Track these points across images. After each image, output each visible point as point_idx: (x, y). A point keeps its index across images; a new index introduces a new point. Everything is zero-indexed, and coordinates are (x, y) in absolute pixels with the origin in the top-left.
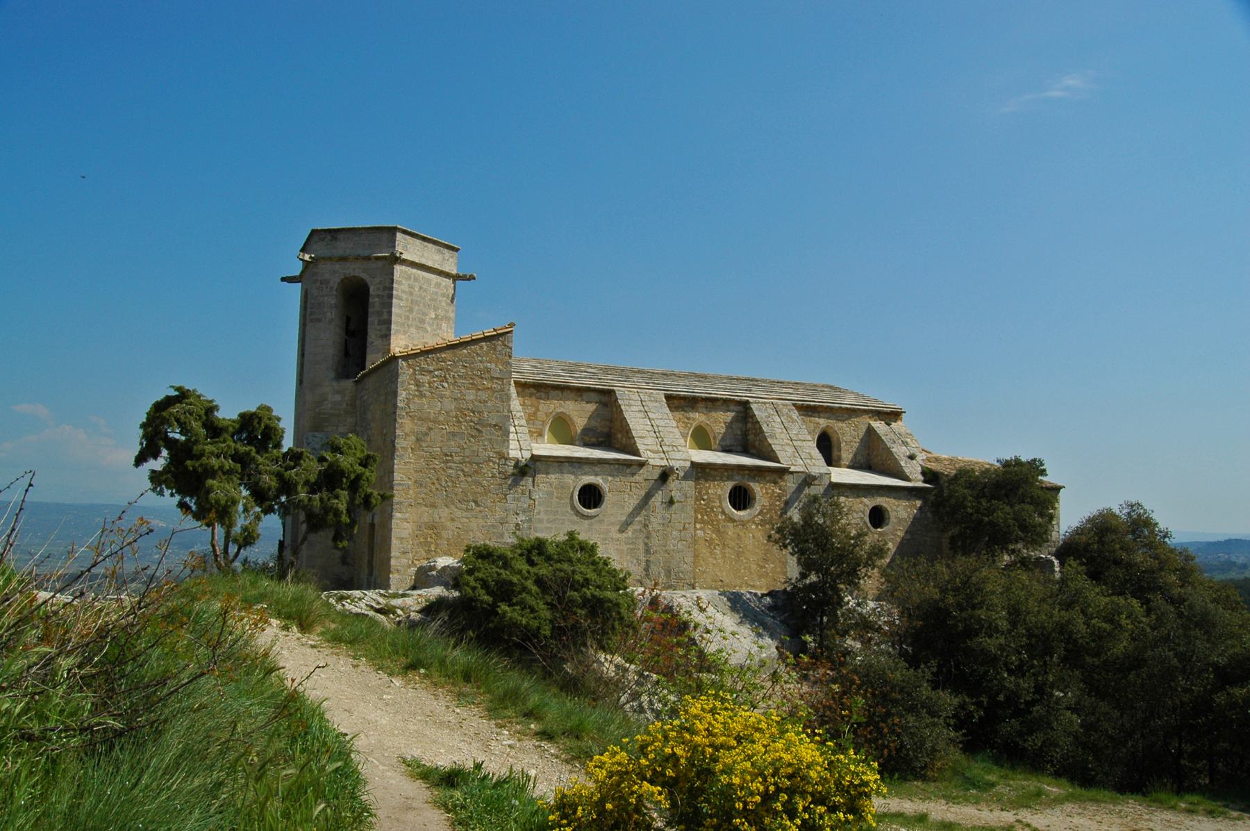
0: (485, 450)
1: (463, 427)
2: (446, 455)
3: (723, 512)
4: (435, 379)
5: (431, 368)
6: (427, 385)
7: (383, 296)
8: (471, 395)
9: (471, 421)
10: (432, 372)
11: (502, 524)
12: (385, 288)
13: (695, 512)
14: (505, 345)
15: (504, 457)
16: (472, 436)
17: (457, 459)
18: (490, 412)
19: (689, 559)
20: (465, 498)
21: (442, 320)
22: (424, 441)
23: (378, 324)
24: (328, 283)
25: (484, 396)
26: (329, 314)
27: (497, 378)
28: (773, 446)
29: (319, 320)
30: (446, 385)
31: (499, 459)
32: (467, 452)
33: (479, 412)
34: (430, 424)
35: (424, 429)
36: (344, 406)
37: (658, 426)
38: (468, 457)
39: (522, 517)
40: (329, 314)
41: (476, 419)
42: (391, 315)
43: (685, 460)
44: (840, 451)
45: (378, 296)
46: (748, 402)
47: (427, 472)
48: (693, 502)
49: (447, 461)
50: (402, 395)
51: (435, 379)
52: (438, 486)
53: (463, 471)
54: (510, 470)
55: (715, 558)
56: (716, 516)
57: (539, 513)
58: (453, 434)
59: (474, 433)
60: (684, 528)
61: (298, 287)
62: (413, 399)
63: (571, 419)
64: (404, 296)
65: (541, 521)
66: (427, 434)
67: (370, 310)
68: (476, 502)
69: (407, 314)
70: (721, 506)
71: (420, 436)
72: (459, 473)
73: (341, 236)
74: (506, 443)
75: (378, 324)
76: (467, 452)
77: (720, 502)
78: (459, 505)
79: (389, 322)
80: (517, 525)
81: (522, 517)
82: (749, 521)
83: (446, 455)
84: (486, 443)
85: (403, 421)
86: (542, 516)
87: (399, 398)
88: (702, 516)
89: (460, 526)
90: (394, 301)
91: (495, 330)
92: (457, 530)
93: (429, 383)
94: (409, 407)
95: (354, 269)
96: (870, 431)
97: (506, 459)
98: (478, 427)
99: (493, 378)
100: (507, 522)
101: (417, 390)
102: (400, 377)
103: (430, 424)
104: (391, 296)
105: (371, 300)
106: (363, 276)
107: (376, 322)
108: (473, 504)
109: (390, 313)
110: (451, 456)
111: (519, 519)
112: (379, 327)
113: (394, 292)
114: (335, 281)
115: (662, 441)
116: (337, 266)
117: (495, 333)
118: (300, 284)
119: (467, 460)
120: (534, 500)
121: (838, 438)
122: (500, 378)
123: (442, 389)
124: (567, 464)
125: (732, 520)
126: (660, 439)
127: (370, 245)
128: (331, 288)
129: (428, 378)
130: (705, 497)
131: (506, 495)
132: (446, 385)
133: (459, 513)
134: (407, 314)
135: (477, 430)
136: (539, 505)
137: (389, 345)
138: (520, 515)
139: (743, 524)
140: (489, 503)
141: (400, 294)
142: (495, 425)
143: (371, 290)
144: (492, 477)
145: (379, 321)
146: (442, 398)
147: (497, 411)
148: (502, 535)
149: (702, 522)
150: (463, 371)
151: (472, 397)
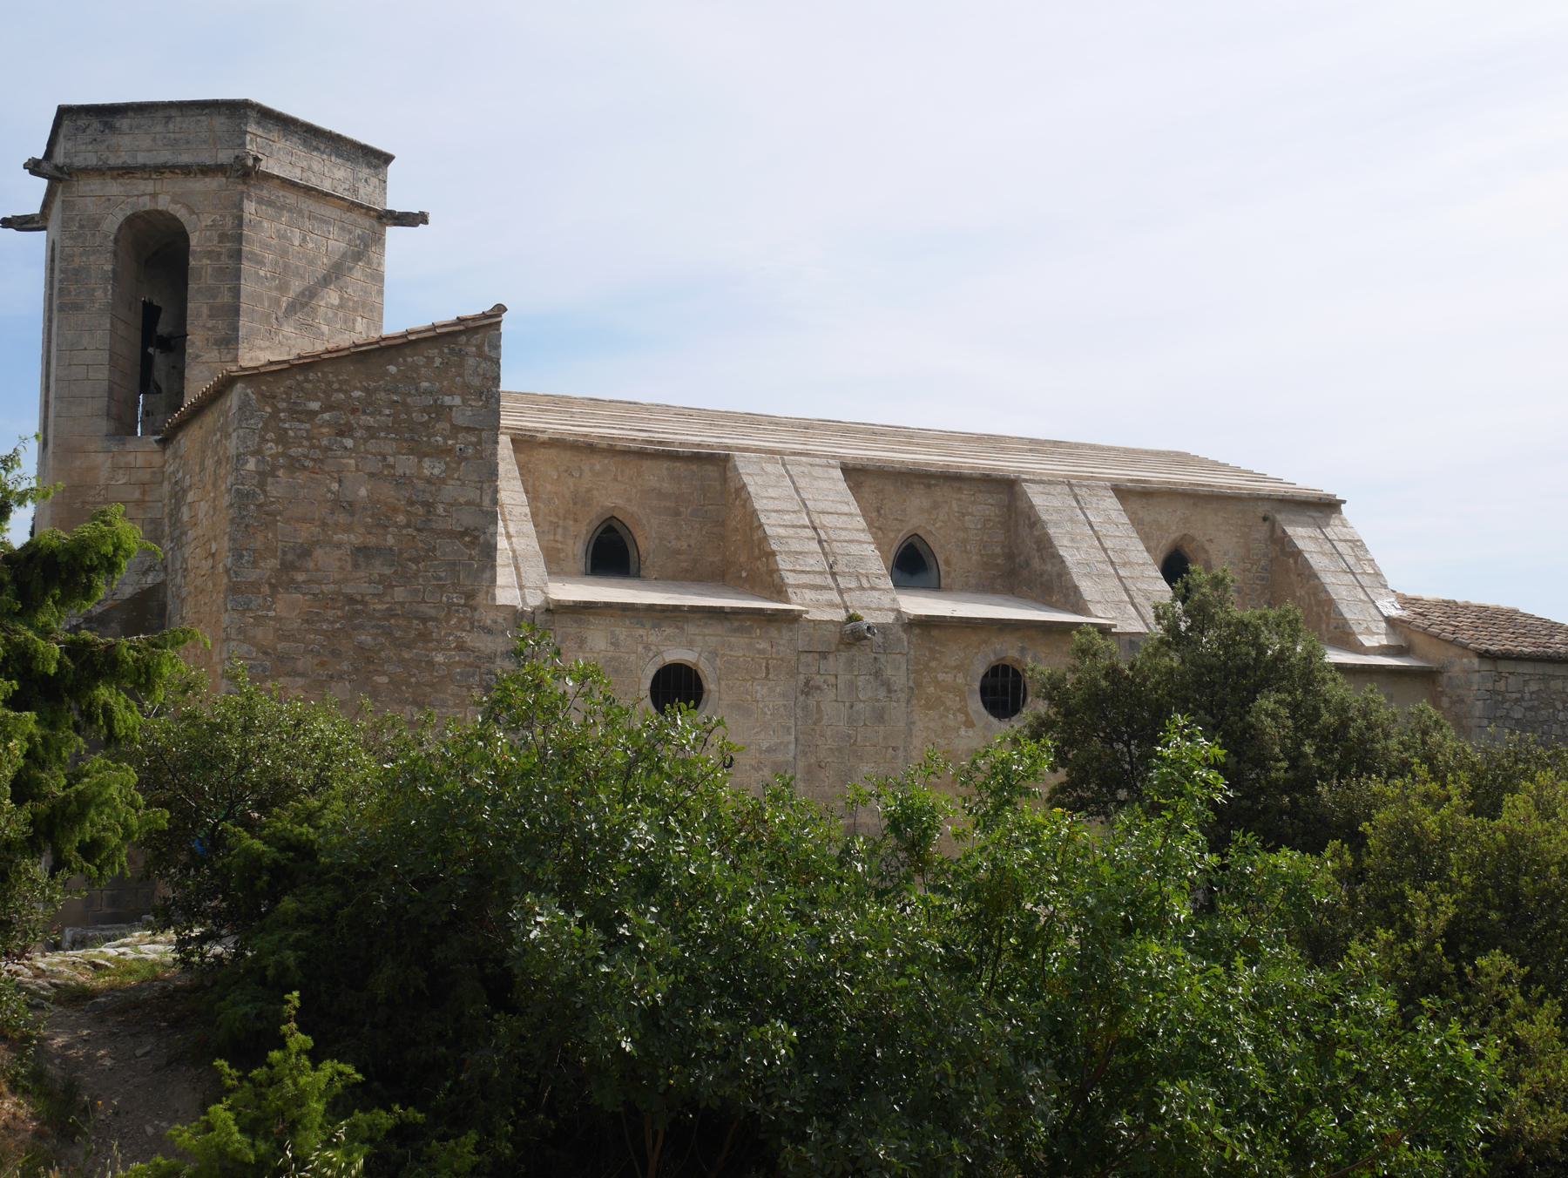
7: (220, 254)
8: (405, 464)
9: (408, 526)
12: (223, 237)
21: (355, 310)
22: (298, 569)
23: (211, 316)
25: (433, 468)
26: (99, 293)
27: (468, 429)
30: (349, 443)
32: (400, 594)
38: (402, 604)
40: (99, 293)
42: (239, 298)
45: (209, 254)
61: (37, 241)
64: (269, 257)
67: (192, 286)
69: (274, 293)
71: (290, 557)
73: (123, 123)
75: (211, 316)
76: (400, 594)
79: (235, 311)
90: (246, 266)
94: (264, 492)
95: (154, 196)
99: (456, 429)
104: (237, 255)
105: (192, 262)
107: (205, 311)
109: (236, 292)
113: (246, 248)
114: (112, 223)
116: (114, 188)
118: (44, 233)
122: (474, 429)
128: (106, 237)
134: (274, 293)
141: (257, 250)
142: (465, 533)
143: (194, 240)
145: (211, 308)
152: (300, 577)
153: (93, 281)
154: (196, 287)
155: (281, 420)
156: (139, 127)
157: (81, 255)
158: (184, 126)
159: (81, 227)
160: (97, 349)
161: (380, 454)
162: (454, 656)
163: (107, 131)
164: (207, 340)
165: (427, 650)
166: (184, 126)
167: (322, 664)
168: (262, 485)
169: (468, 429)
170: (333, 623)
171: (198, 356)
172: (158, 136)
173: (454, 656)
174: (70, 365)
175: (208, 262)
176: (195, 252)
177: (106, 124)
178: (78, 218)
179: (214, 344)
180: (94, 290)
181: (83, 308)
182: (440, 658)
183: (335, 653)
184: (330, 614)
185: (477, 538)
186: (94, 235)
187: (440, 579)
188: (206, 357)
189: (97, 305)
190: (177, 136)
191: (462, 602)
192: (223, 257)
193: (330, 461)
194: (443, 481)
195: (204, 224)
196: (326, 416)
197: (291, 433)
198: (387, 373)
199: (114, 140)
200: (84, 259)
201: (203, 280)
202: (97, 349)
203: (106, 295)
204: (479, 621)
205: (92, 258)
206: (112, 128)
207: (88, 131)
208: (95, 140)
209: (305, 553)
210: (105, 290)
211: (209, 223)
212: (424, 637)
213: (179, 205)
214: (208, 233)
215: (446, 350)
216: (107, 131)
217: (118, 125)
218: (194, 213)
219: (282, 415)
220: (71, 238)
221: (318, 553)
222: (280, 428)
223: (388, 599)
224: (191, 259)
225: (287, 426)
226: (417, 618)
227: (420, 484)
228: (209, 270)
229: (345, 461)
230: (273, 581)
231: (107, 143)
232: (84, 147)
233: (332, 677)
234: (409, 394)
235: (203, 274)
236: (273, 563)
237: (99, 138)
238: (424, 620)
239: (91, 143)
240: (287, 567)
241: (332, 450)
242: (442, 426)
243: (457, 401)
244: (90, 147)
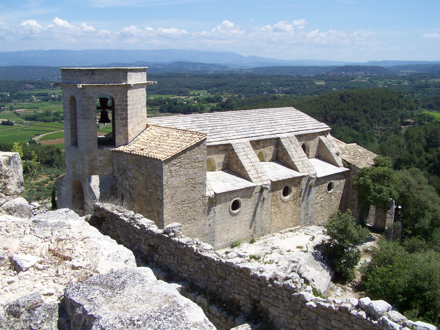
0: (197, 195)
1: (189, 187)
2: (183, 201)
3: (281, 199)
4: (177, 168)
5: (175, 163)
6: (174, 171)
9: (192, 184)
10: (176, 164)
11: (204, 226)
12: (123, 101)
13: (272, 202)
14: (204, 145)
15: (204, 196)
16: (192, 190)
17: (187, 202)
19: (269, 222)
20: (190, 219)
23: (121, 120)
24: (92, 98)
25: (196, 170)
28: (295, 163)
29: (89, 118)
30: (181, 169)
31: (203, 198)
32: (191, 198)
33: (195, 179)
34: (176, 189)
35: (174, 192)
36: (106, 162)
37: (253, 162)
38: (191, 200)
39: (211, 221)
41: (193, 182)
43: (268, 180)
44: (309, 152)
45: (120, 105)
46: (279, 138)
47: (176, 211)
48: (271, 198)
49: (183, 204)
50: (165, 178)
51: (177, 168)
52: (180, 216)
53: (189, 207)
54: (207, 201)
55: (277, 219)
56: (278, 201)
57: (217, 217)
58: (185, 191)
59: (193, 188)
60: (268, 210)
62: (169, 179)
63: (213, 160)
65: (218, 220)
66: (175, 194)
68: (194, 219)
70: (280, 197)
71: (173, 195)
72: (188, 208)
77: (280, 195)
78: (188, 222)
79: (127, 119)
80: (210, 224)
81: (211, 221)
82: (289, 201)
85: (166, 191)
86: (219, 218)
87: (164, 180)
88: (274, 203)
89: (189, 231)
91: (200, 139)
92: (188, 233)
93: (175, 170)
94: (168, 183)
95: (106, 91)
96: (320, 141)
97: (205, 197)
98: (194, 185)
101: (170, 175)
102: (164, 170)
103: (176, 189)
104: (127, 106)
108: (193, 220)
109: (127, 114)
110: (185, 201)
111: (210, 222)
115: (257, 171)
117: (200, 140)
119: (190, 202)
120: (215, 212)
121: (309, 146)
123: (180, 172)
124: (228, 194)
125: (283, 202)
126: (256, 170)
127: (113, 78)
130: (275, 195)
132: (181, 169)
133: (188, 225)
135: (194, 187)
136: (218, 214)
137: (127, 130)
139: (287, 202)
140: (199, 218)
142: (201, 183)
144: (200, 206)
146: (180, 176)
147: (201, 177)
148: (204, 230)
149: (274, 205)
150: (188, 161)
151: (192, 173)
159: (88, 99)
194: (197, 173)
206: (94, 74)
224: (115, 106)
243: (199, 156)
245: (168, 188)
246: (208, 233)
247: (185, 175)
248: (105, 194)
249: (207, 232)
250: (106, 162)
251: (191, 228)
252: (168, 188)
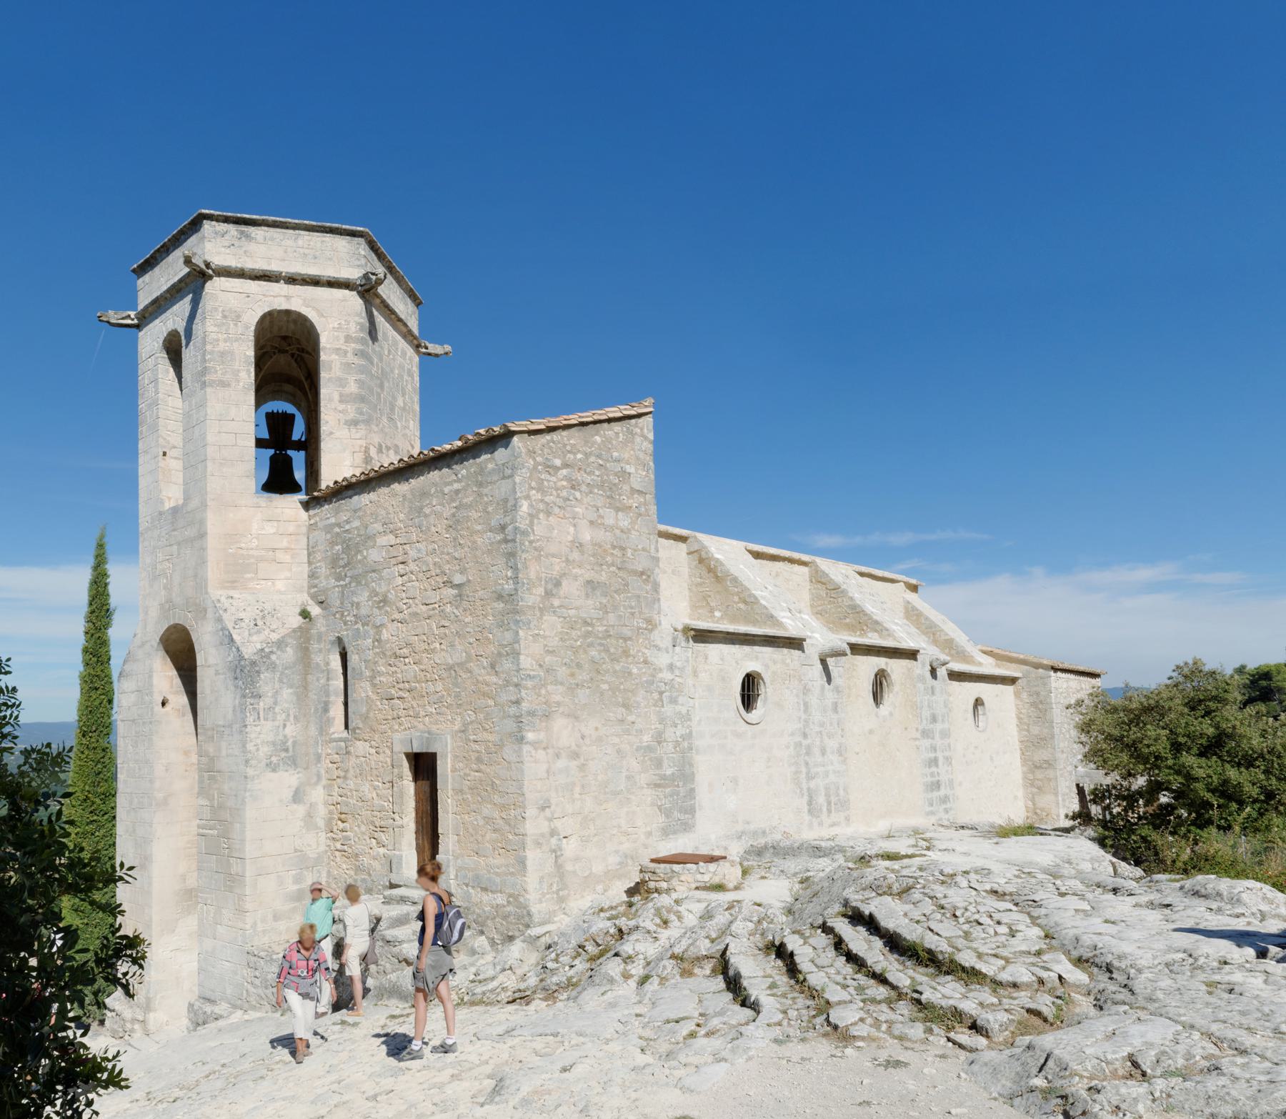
2: (586, 623)
4: (565, 483)
7: (346, 352)
8: (610, 517)
11: (659, 743)
18: (635, 550)
23: (341, 401)
25: (624, 522)
27: (640, 492)
30: (578, 494)
38: (613, 626)
40: (243, 375)
49: (588, 634)
71: (550, 586)
72: (603, 655)
74: (656, 606)
75: (341, 401)
76: (612, 618)
83: (586, 623)
84: (633, 604)
99: (633, 491)
100: (665, 741)
106: (305, 311)
107: (336, 397)
112: (341, 407)
122: (642, 492)
129: (554, 479)
131: (661, 693)
138: (679, 727)
142: (642, 573)
145: (341, 395)
148: (659, 764)
150: (597, 473)
152: (556, 603)
153: (237, 364)
154: (327, 376)
155: (540, 472)
156: (272, 239)
157: (225, 341)
158: (311, 243)
159: (225, 317)
160: (244, 421)
161: (595, 506)
162: (642, 668)
163: (243, 239)
164: (339, 420)
165: (627, 663)
166: (311, 243)
167: (572, 675)
168: (531, 524)
169: (640, 492)
170: (576, 641)
171: (331, 433)
172: (289, 249)
173: (642, 668)
174: (220, 432)
175: (337, 357)
176: (325, 348)
177: (242, 232)
178: (221, 309)
179: (345, 424)
180: (238, 371)
181: (229, 385)
182: (635, 671)
183: (579, 666)
184: (574, 633)
185: (649, 576)
186: (236, 325)
187: (632, 608)
188: (338, 434)
189: (241, 384)
190: (307, 251)
191: (645, 626)
192: (349, 355)
193: (569, 508)
195: (331, 326)
196: (564, 472)
197: (546, 483)
198: (595, 442)
199: (252, 247)
200: (228, 344)
201: (333, 371)
202: (244, 421)
203: (249, 376)
204: (653, 641)
205: (236, 345)
207: (227, 237)
208: (233, 245)
209: (558, 584)
210: (248, 371)
211: (336, 326)
212: (626, 653)
213: (310, 309)
214: (336, 333)
215: (625, 429)
216: (243, 239)
217: (253, 235)
218: (323, 316)
219: (540, 467)
220: (216, 325)
221: (564, 583)
222: (540, 479)
223: (605, 623)
224: (322, 353)
225: (543, 477)
226: (621, 638)
227: (618, 532)
228: (338, 363)
229: (577, 509)
230: (541, 606)
231: (244, 249)
232: (223, 249)
233: (577, 685)
234: (608, 461)
235: (333, 366)
236: (541, 591)
237: (236, 243)
238: (626, 639)
239: (229, 247)
240: (548, 594)
241: (569, 500)
242: (626, 487)
244: (228, 251)
245: (536, 549)
246: (673, 774)
247: (592, 523)
248: (278, 648)
249: (669, 772)
250: (285, 544)
251: (616, 740)
252: (536, 549)
